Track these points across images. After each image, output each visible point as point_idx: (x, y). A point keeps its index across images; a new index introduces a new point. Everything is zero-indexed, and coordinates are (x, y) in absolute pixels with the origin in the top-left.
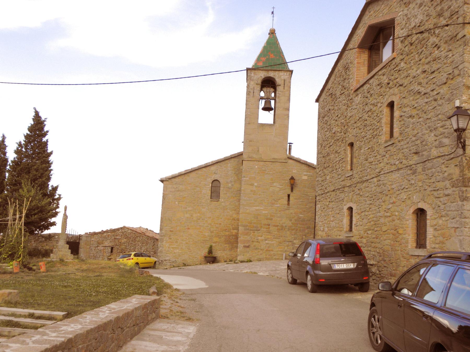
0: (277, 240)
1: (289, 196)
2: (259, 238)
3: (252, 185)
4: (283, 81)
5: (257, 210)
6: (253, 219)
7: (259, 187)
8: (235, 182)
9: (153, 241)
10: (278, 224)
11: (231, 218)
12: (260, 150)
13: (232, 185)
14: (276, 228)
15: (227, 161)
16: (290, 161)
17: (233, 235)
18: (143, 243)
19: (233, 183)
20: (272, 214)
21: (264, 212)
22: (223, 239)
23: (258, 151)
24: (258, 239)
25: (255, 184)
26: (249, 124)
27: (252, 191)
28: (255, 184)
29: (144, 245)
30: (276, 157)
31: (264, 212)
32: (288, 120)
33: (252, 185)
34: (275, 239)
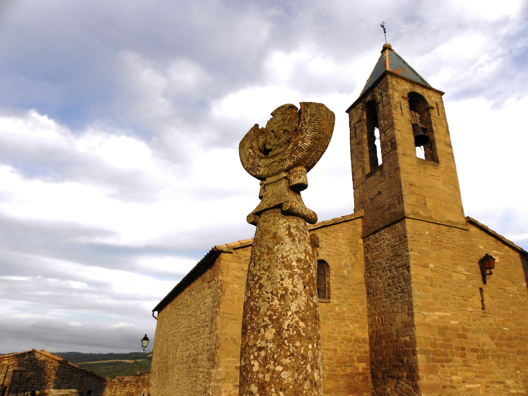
0: (483, 380)
1: (481, 289)
2: (454, 377)
3: (426, 266)
4: (435, 104)
5: (441, 318)
6: (437, 337)
7: (436, 271)
8: (352, 266)
9: (81, 375)
10: (477, 347)
11: (353, 338)
12: (428, 204)
13: (349, 272)
14: (476, 355)
15: (336, 227)
16: (473, 229)
17: (359, 374)
18: (64, 379)
19: (350, 269)
20: (466, 326)
21: (452, 322)
22: (342, 383)
23: (425, 204)
24: (451, 381)
25: (431, 266)
26: (404, 155)
27: (427, 278)
28: (431, 266)
29: (65, 381)
30: (452, 220)
31: (452, 322)
32: (454, 162)
33: (426, 266)
34: (478, 380)
